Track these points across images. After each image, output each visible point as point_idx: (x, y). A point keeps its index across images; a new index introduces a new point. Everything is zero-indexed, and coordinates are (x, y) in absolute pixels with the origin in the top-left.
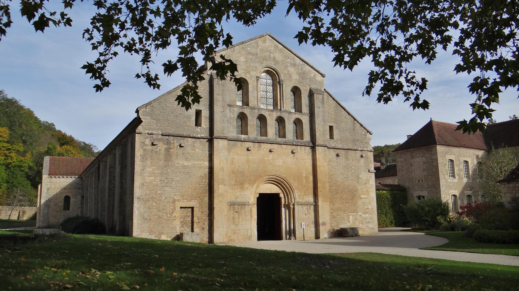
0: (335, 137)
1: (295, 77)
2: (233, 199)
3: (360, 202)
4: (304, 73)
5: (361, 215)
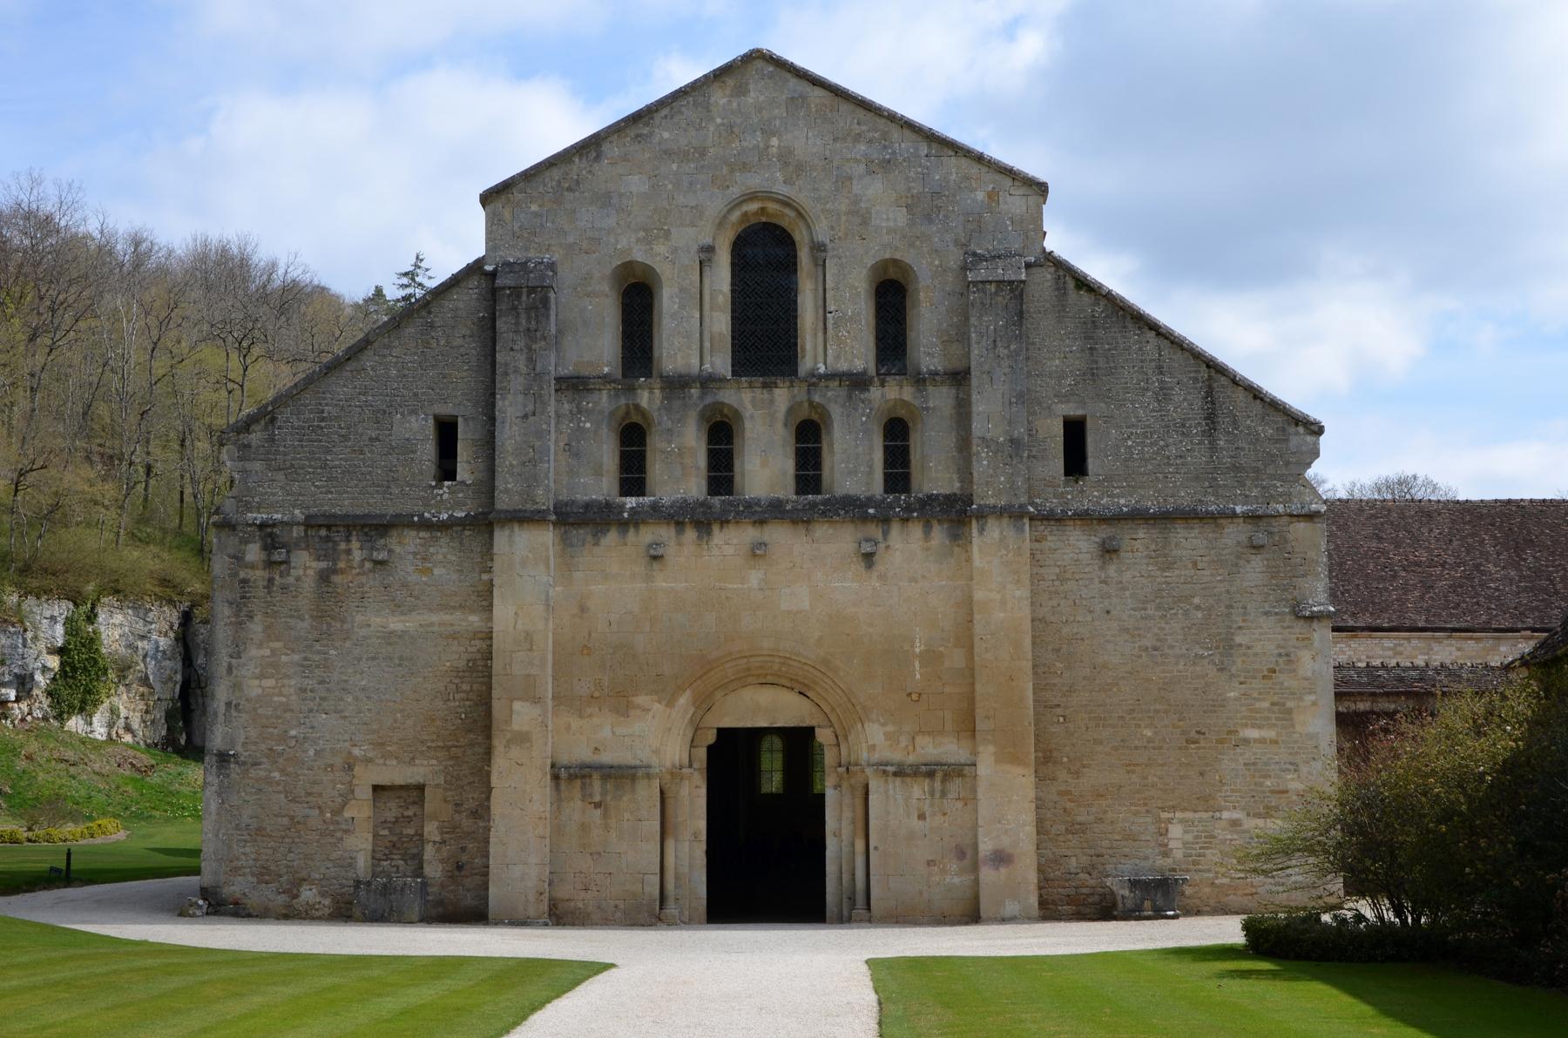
0: (1092, 464)
1: (889, 216)
2: (581, 753)
4: (936, 194)
5: (1235, 823)
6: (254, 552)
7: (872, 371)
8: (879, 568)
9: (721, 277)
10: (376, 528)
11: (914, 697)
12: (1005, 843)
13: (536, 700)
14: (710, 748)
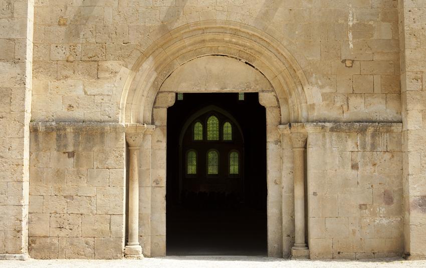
11: (348, 63)
14: (170, 110)
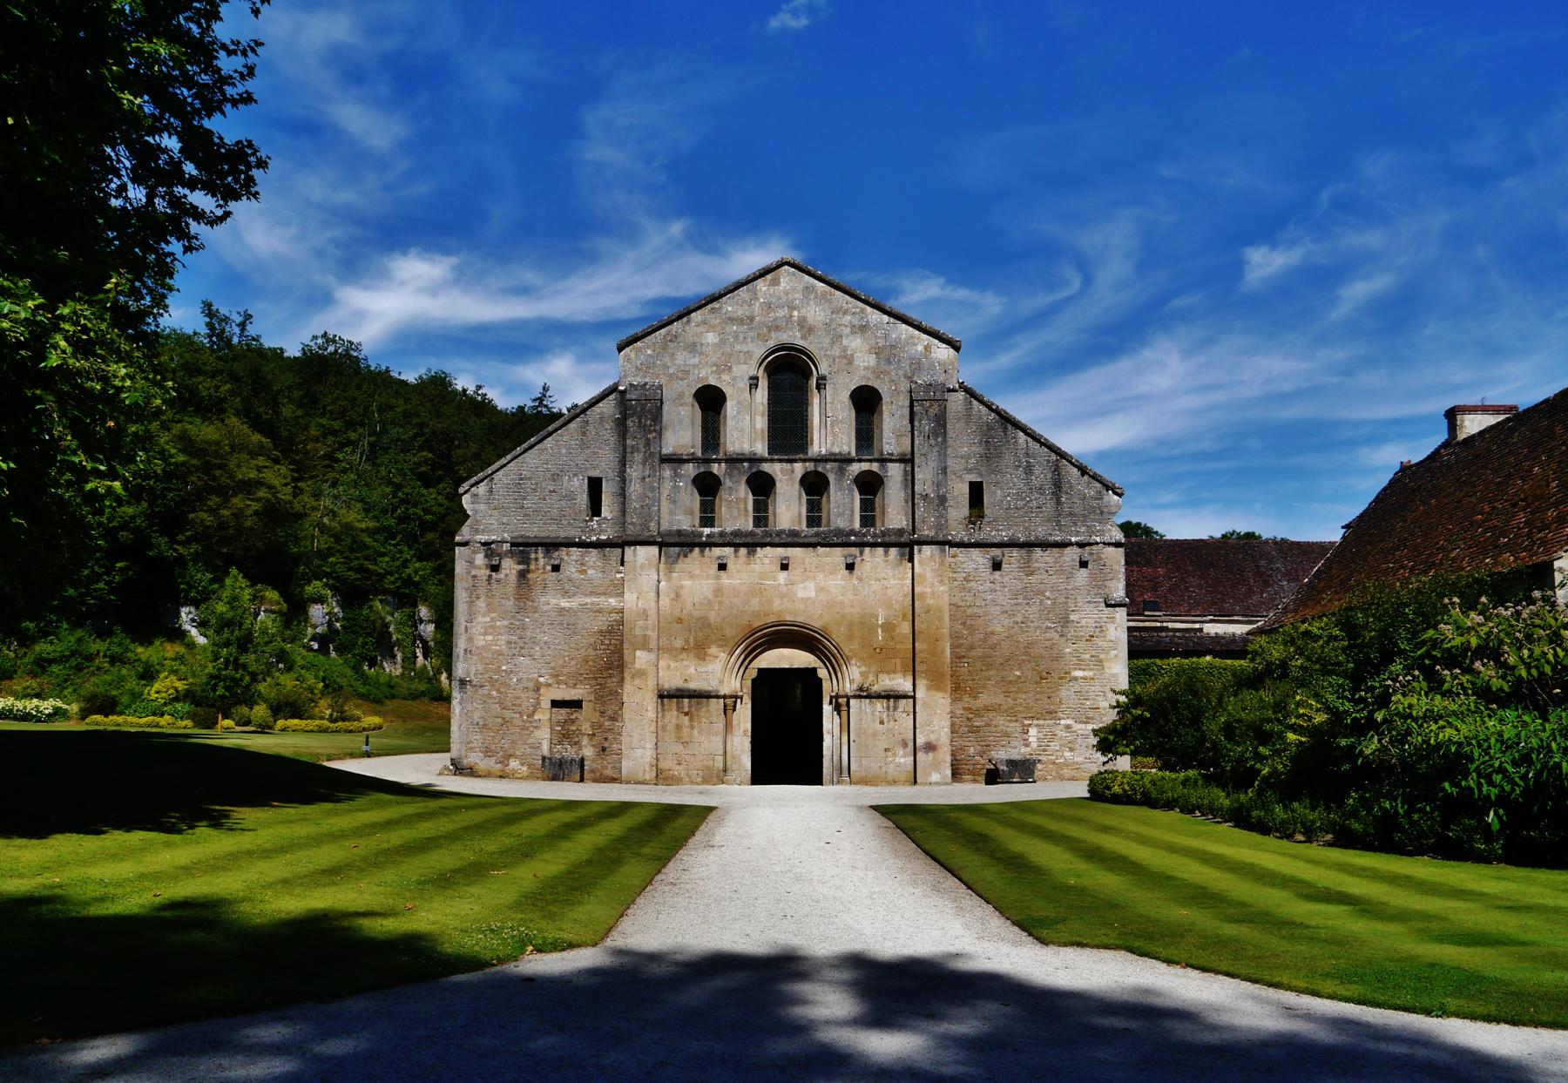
3: (1067, 693)
5: (1068, 727)
6: (480, 559)
7: (853, 454)
8: (857, 571)
9: (762, 395)
10: (551, 546)
12: (932, 738)
13: (650, 650)
